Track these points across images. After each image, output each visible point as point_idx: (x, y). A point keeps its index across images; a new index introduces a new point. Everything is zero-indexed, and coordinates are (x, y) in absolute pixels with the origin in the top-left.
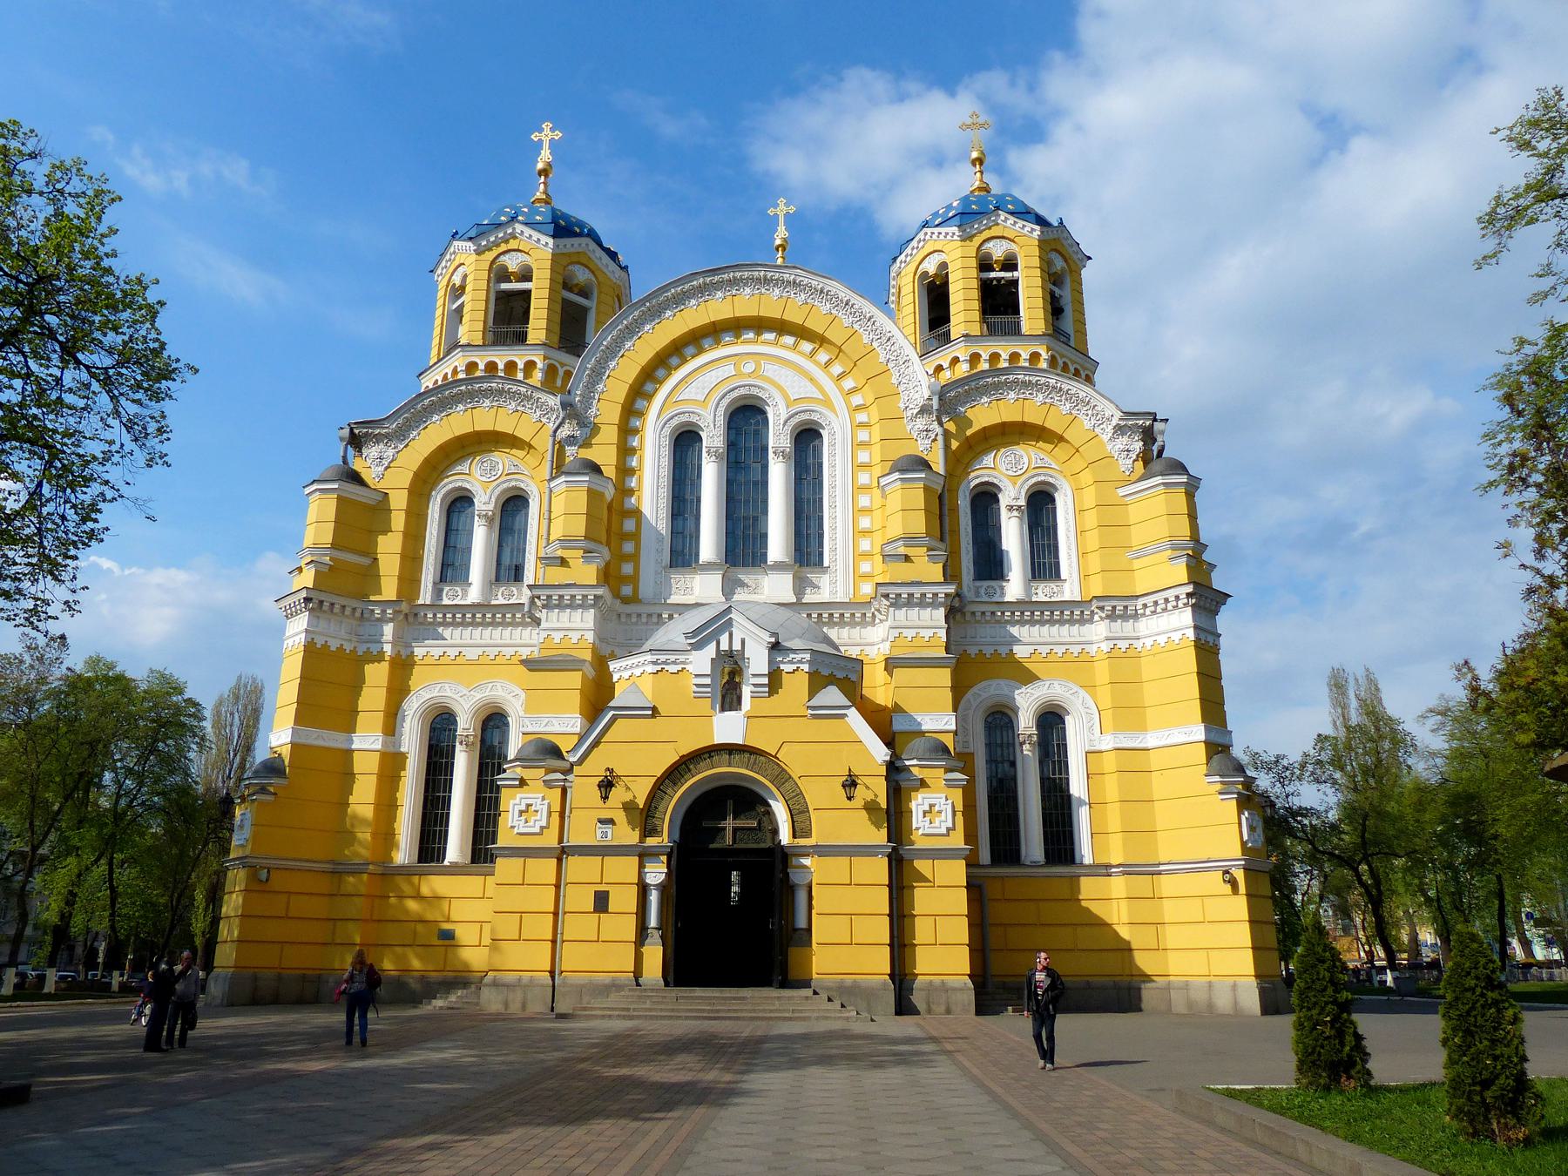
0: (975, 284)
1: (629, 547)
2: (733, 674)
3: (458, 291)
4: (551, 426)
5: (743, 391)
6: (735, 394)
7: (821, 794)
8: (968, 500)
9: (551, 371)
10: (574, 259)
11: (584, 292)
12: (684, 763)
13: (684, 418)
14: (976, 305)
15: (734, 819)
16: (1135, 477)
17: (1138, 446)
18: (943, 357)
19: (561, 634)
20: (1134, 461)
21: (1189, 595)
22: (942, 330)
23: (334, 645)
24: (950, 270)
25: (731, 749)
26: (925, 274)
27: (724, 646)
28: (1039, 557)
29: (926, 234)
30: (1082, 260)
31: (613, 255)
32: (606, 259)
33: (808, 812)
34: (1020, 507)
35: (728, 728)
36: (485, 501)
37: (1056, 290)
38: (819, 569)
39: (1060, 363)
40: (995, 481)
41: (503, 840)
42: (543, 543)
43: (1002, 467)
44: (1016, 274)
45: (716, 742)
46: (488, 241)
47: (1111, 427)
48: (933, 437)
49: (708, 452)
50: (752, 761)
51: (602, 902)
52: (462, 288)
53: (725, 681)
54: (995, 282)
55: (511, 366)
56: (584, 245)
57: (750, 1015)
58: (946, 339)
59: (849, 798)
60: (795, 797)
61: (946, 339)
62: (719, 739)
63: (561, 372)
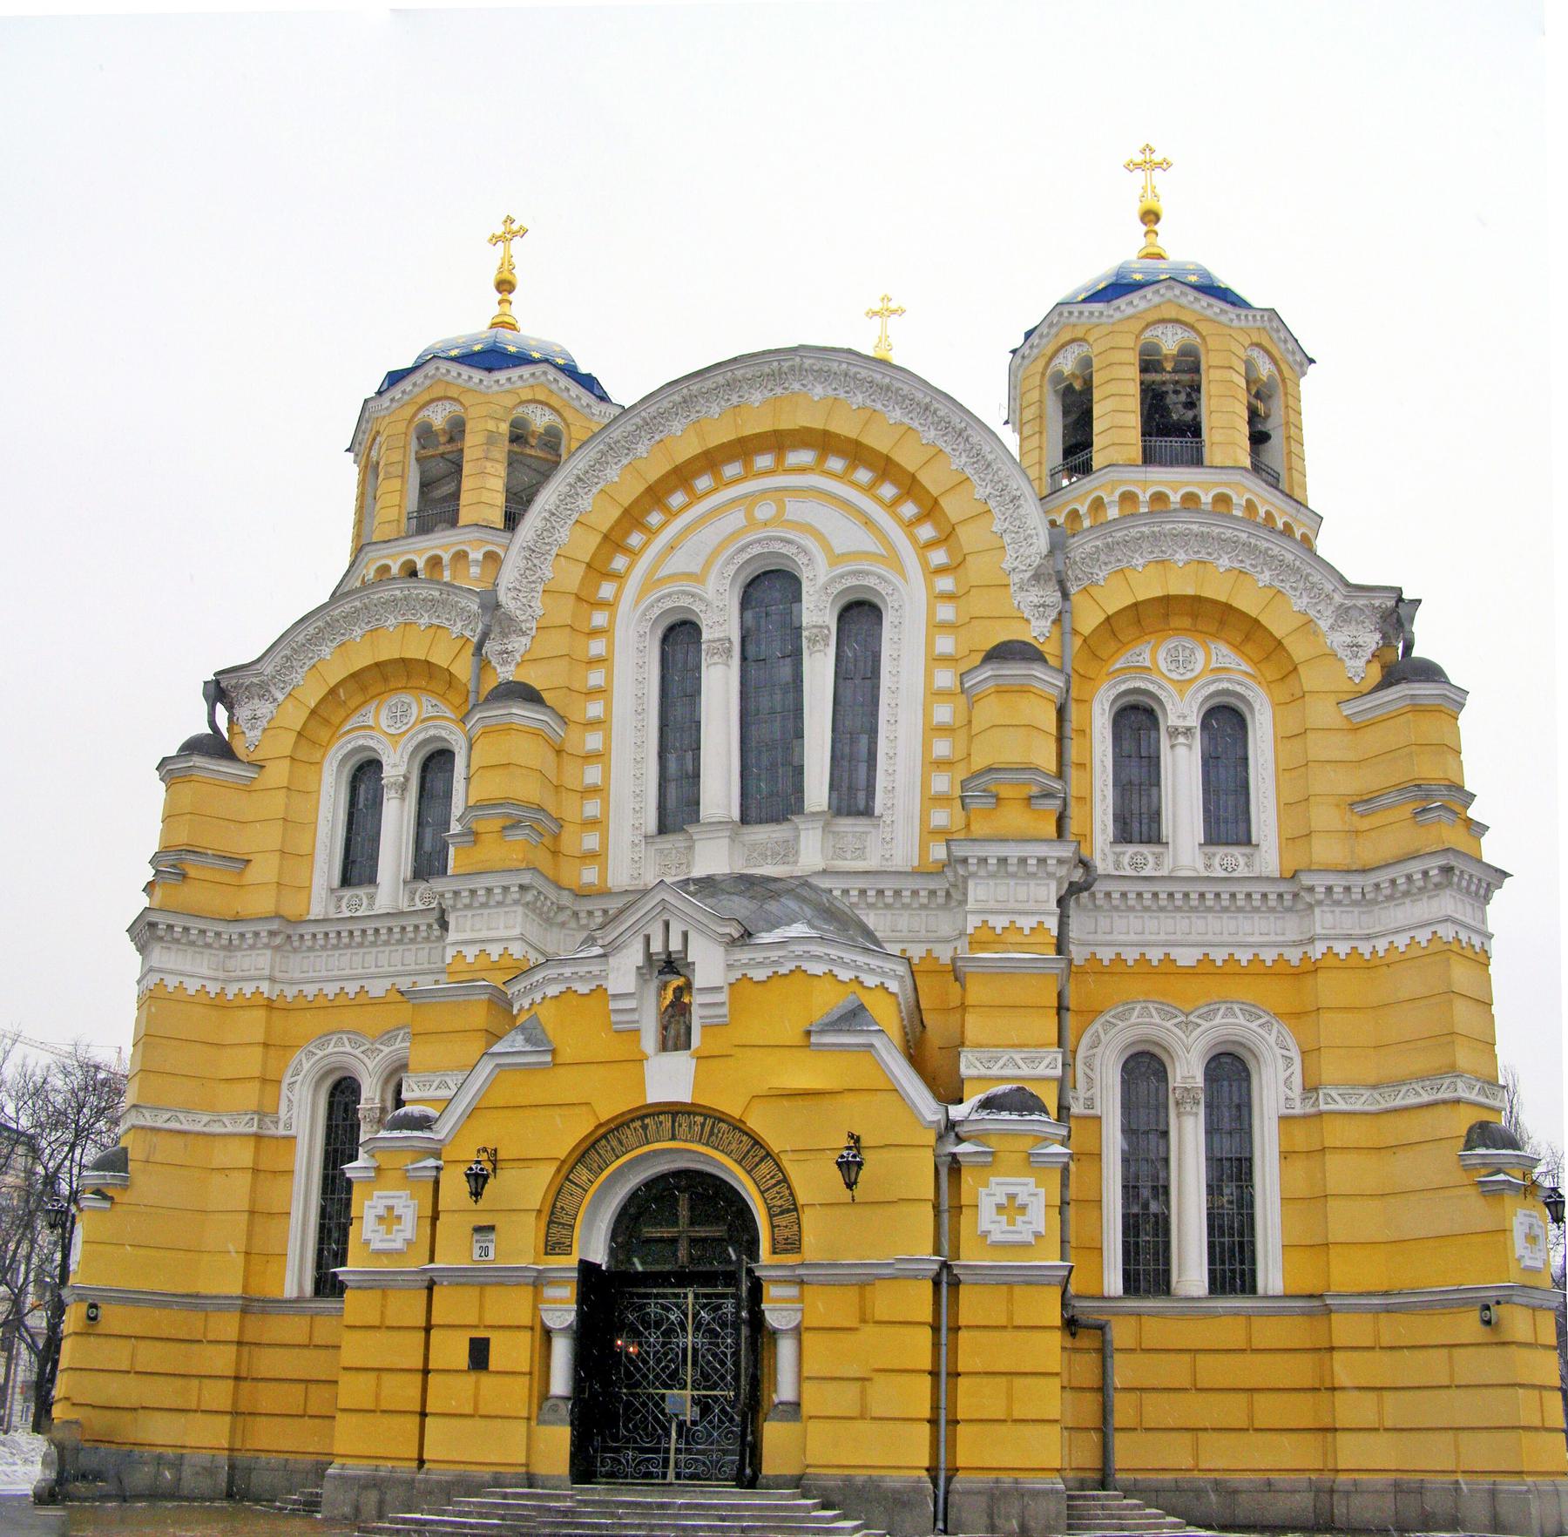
4: (475, 640)
12: (604, 1136)
18: (1078, 493)
22: (1078, 459)
25: (675, 1110)
26: (1058, 377)
33: (796, 1209)
45: (650, 1101)
50: (707, 1129)
58: (1085, 469)
59: (850, 1185)
60: (775, 1185)
61: (1085, 469)
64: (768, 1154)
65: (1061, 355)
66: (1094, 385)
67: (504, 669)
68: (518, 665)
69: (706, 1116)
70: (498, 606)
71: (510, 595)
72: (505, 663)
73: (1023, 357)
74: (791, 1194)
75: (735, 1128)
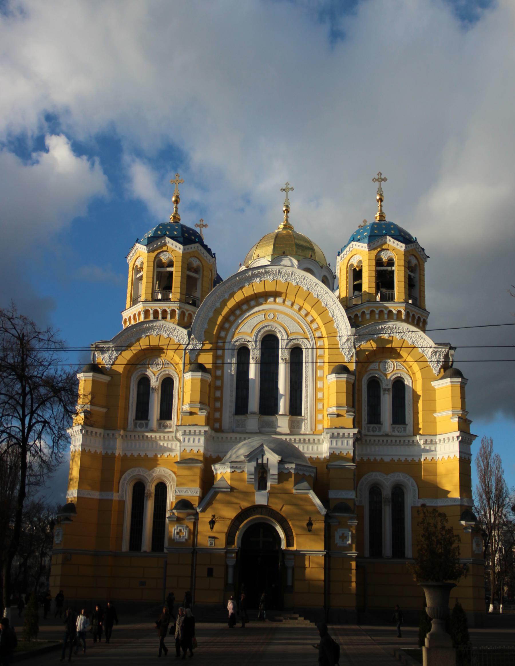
1: (218, 405)
3: (138, 270)
9: (182, 314)
11: (196, 271)
21: (458, 437)
26: (352, 265)
30: (425, 259)
31: (209, 251)
32: (206, 254)
37: (412, 275)
39: (411, 315)
48: (352, 354)
49: (253, 358)
51: (210, 573)
52: (142, 268)
55: (164, 312)
56: (196, 247)
63: (187, 314)
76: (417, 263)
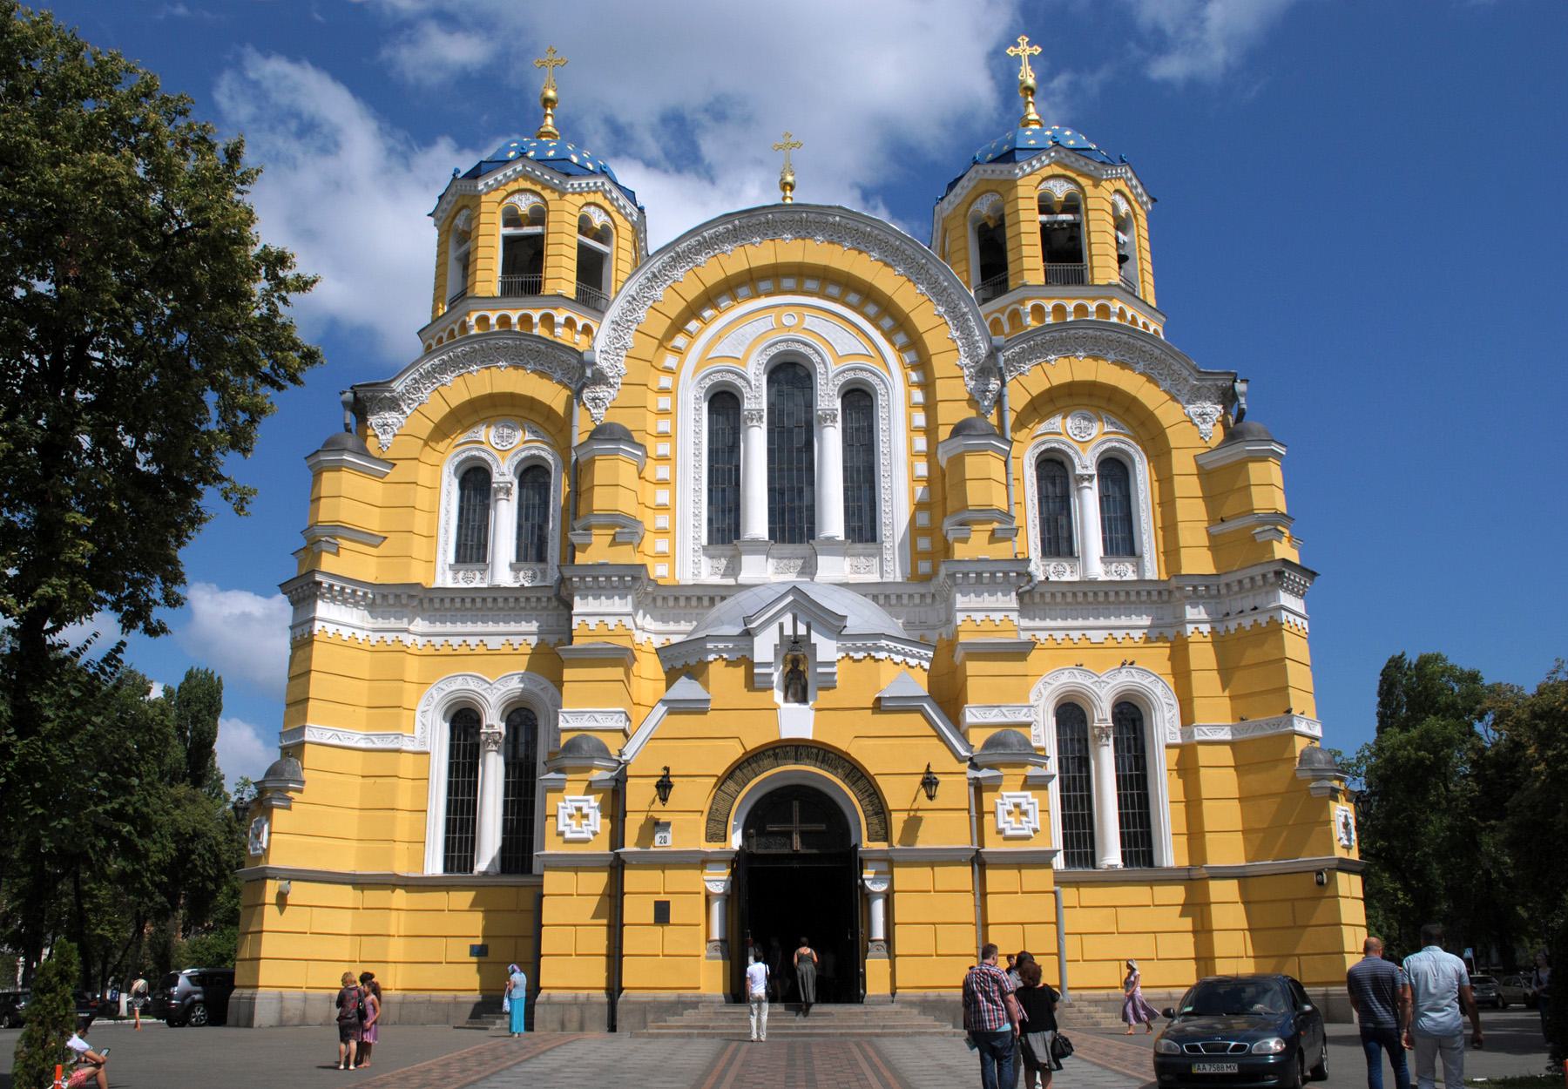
0: (1037, 228)
2: (795, 662)
5: (782, 347)
6: (774, 351)
7: (899, 794)
8: (1033, 468)
10: (591, 198)
11: (603, 235)
12: (747, 760)
13: (718, 378)
14: (1038, 251)
15: (801, 822)
16: (1214, 443)
17: (1215, 410)
19: (596, 620)
20: (1214, 425)
23: (346, 633)
24: (1007, 212)
26: (975, 219)
27: (788, 631)
28: (1111, 532)
29: (977, 172)
33: (883, 812)
34: (1091, 477)
35: (797, 721)
36: (504, 472)
38: (870, 545)
40: (1063, 447)
41: (551, 847)
42: (571, 517)
43: (1070, 431)
44: (1077, 217)
46: (496, 180)
47: (1188, 388)
50: (820, 758)
51: (662, 913)
53: (788, 669)
54: (1056, 226)
55: (526, 320)
57: (839, 1031)
59: (931, 797)
62: (785, 736)
64: (863, 775)
65: (979, 200)
66: (1007, 225)
67: (596, 411)
68: (607, 409)
69: (819, 749)
70: (595, 364)
71: (604, 356)
72: (597, 406)
73: (949, 203)
74: (880, 803)
75: (840, 757)
76: (1129, 208)
